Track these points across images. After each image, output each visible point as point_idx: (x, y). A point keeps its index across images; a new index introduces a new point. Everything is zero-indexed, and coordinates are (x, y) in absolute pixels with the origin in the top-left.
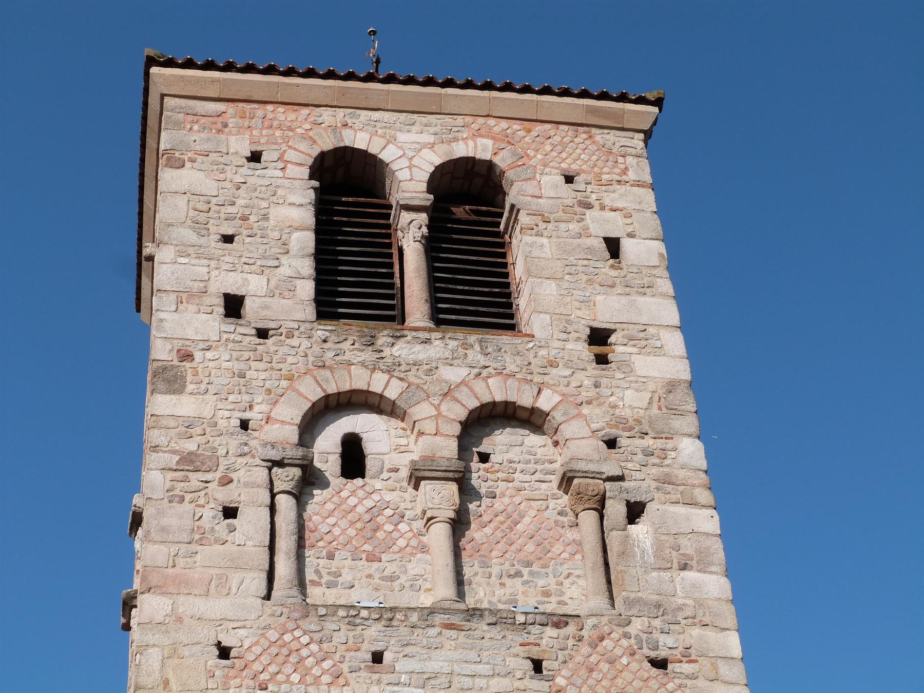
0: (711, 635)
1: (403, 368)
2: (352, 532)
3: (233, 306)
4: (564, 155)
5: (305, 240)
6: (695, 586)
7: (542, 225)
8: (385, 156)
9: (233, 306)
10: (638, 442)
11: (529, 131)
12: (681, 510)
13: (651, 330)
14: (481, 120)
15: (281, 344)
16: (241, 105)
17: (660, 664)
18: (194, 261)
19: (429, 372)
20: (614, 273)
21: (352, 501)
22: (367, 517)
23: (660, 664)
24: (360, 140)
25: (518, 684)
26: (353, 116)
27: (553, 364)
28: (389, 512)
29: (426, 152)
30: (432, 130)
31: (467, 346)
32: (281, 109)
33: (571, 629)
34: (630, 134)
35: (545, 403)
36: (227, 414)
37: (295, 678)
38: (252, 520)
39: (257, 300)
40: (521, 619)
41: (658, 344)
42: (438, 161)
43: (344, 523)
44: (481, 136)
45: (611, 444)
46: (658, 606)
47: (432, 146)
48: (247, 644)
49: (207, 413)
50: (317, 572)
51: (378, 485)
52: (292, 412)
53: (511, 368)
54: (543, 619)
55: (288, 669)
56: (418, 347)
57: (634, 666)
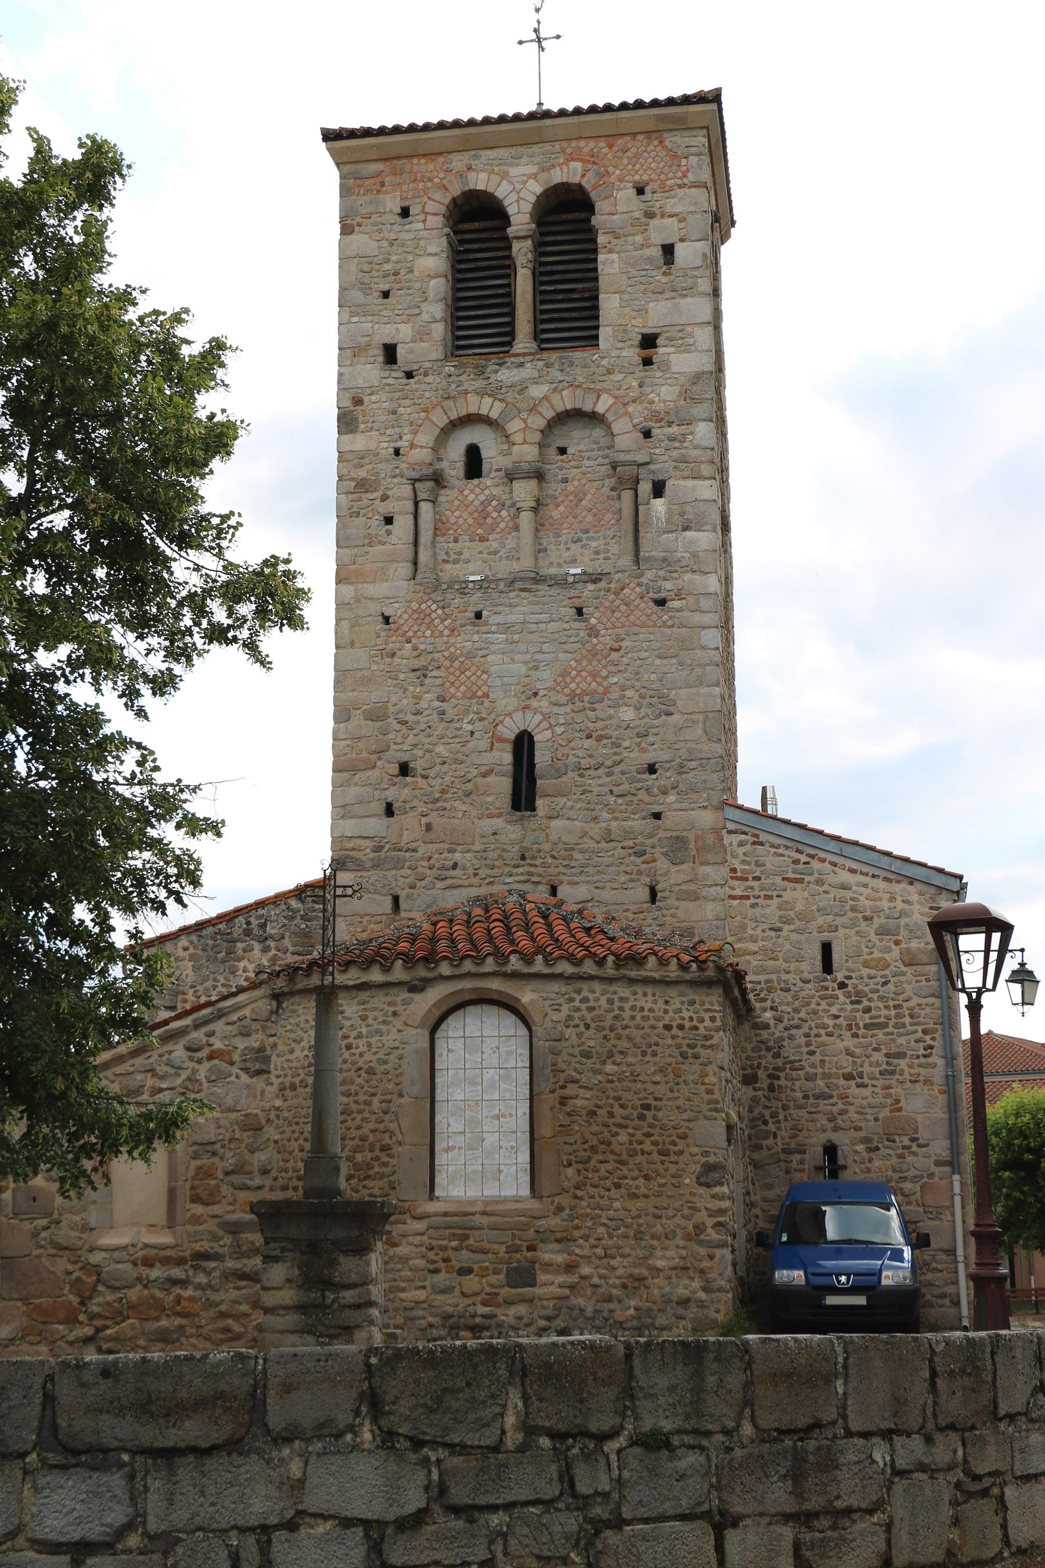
0: (697, 577)
1: (504, 390)
2: (470, 521)
3: (390, 353)
4: (637, 167)
5: (438, 287)
6: (693, 542)
7: (614, 241)
8: (500, 194)
9: (390, 353)
10: (666, 430)
11: (610, 146)
12: (690, 483)
13: (689, 329)
14: (574, 144)
15: (419, 382)
16: (395, 162)
17: (661, 603)
18: (363, 319)
19: (521, 392)
20: (664, 279)
21: (472, 497)
22: (481, 508)
23: (661, 603)
24: (480, 181)
25: (565, 626)
26: (476, 157)
27: (610, 372)
28: (495, 503)
29: (531, 181)
30: (538, 159)
31: (548, 365)
32: (423, 161)
33: (602, 584)
34: (694, 132)
35: (600, 409)
36: (385, 445)
37: (428, 633)
38: (403, 524)
39: (406, 346)
40: (571, 579)
41: (691, 341)
42: (539, 190)
43: (465, 515)
44: (573, 160)
45: (647, 434)
46: (665, 560)
47: (534, 176)
48: (399, 613)
49: (373, 446)
50: (447, 553)
51: (489, 483)
52: (426, 438)
53: (580, 379)
54: (586, 578)
55: (424, 627)
56: (515, 372)
57: (643, 605)
